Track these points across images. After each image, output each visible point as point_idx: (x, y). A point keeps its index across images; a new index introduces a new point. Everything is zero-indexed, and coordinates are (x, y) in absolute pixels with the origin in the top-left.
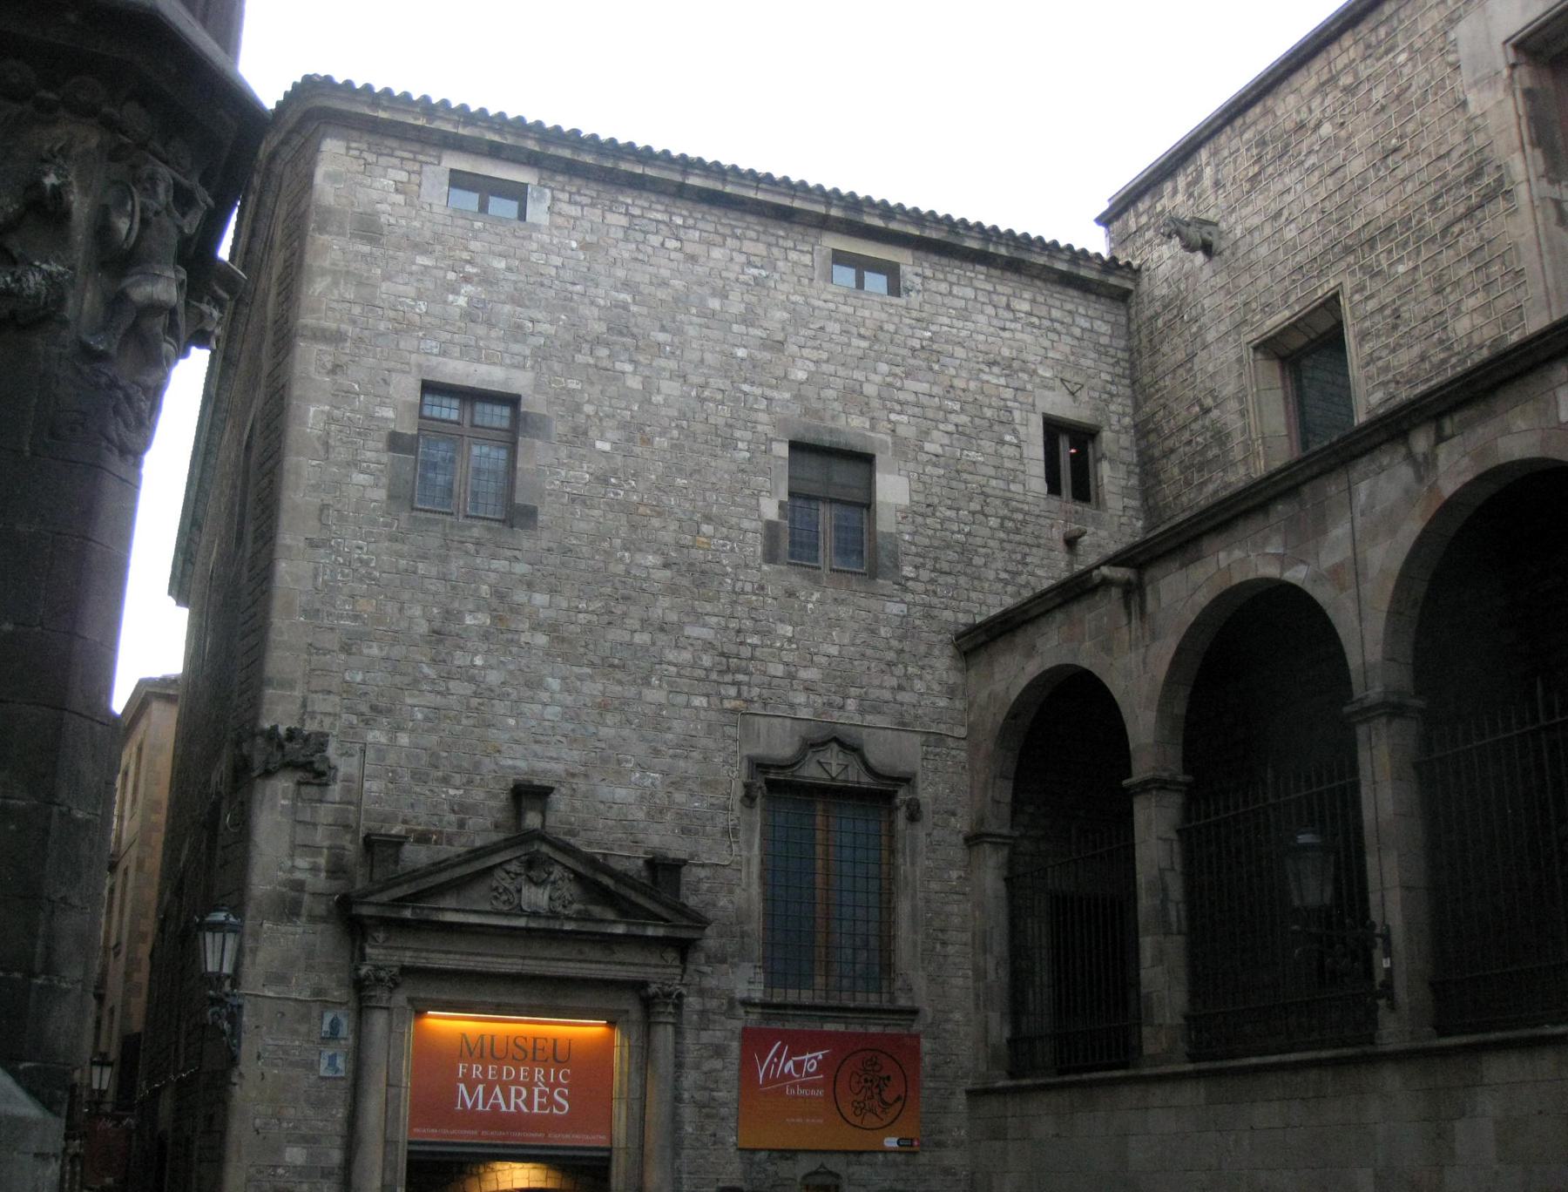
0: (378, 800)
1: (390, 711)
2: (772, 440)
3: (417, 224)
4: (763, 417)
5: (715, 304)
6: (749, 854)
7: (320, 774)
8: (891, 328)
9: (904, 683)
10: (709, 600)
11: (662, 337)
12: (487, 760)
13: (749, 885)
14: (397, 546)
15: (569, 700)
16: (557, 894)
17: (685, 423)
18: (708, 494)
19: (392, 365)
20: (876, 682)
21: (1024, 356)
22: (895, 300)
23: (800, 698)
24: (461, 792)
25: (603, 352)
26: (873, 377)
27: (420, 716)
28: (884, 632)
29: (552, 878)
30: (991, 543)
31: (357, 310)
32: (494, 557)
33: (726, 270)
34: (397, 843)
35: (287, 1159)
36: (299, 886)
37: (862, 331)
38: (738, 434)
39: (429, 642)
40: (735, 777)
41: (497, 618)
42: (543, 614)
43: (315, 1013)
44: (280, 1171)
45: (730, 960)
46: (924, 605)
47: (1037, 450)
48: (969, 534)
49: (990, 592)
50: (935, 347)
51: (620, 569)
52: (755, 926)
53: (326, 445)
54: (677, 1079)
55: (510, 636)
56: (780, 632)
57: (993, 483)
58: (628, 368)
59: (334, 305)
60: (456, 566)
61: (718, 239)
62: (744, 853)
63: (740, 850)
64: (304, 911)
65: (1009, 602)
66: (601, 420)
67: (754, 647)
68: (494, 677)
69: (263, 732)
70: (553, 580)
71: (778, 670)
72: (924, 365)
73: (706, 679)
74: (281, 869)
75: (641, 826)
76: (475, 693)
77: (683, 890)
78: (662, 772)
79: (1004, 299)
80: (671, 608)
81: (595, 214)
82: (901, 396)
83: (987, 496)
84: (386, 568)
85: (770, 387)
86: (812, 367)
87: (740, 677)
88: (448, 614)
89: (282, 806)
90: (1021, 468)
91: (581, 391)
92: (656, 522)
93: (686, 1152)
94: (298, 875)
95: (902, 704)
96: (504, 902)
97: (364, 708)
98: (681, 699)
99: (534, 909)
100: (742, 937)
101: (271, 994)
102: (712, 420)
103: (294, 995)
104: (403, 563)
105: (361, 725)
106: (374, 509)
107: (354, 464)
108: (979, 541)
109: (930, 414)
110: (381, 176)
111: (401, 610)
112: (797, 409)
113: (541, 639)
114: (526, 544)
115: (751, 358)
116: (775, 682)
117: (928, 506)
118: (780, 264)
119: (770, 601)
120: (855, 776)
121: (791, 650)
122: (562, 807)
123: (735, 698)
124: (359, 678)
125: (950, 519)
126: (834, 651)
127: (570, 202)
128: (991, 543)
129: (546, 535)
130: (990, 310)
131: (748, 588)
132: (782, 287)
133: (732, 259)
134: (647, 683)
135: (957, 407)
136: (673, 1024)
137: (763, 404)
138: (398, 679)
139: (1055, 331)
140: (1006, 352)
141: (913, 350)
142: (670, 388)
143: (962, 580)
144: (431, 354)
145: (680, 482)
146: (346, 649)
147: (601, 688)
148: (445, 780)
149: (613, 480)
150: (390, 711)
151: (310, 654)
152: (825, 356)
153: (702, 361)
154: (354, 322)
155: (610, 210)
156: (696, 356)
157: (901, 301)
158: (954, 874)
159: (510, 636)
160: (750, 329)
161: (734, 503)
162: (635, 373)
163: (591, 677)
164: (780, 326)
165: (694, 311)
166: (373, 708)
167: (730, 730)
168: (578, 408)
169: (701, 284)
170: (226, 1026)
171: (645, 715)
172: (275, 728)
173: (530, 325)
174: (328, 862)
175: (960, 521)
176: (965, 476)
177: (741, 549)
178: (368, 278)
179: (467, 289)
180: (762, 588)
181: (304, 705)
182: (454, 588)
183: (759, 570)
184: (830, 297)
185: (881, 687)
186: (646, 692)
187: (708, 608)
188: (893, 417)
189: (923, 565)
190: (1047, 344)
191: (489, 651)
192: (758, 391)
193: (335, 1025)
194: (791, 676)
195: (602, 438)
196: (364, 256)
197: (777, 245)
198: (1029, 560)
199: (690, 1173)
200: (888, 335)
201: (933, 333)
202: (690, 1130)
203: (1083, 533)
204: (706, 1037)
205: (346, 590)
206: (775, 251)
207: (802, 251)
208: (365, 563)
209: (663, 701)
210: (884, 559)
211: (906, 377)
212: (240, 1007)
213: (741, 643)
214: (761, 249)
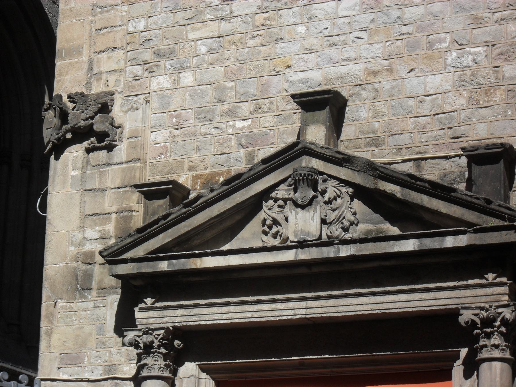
7: (102, 136)
16: (332, 216)
24: (249, 122)
27: (203, 49)
64: (94, 285)
74: (72, 244)
75: (462, 116)
78: (486, 44)
89: (73, 177)
105: (146, 74)
138: (180, 15)
148: (231, 113)
166: (159, 54)
174: (116, 228)
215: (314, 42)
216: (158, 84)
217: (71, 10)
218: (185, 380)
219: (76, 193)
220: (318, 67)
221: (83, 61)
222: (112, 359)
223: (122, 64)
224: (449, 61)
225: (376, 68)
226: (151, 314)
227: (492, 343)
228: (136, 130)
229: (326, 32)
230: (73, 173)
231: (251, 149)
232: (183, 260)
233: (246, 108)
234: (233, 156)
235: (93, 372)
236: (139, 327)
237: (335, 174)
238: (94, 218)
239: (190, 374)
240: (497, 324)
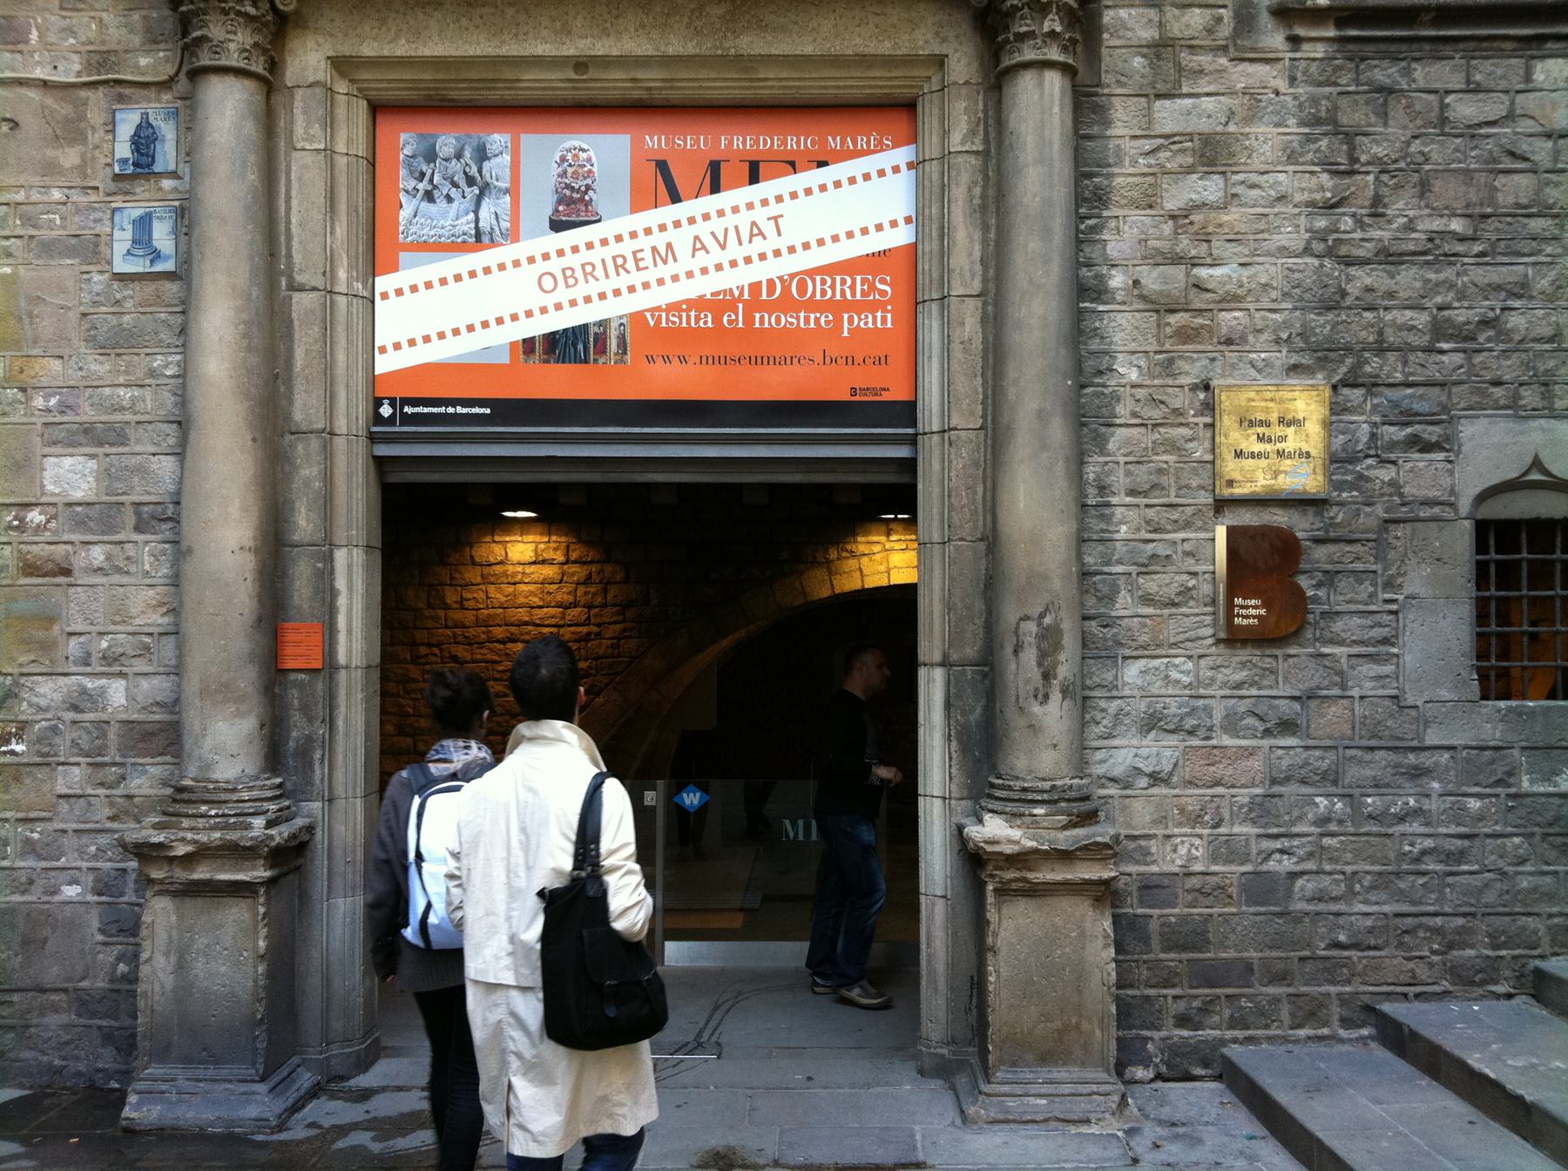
35: (50, 487)
43: (95, 116)
44: (35, 516)
93: (1121, 433)
103: (39, 73)
136: (1065, 68)
193: (144, 141)
199: (1132, 492)
202: (1134, 375)
204: (1169, 115)
218: (299, 94)
222: (107, 38)
227: (1046, 29)
235: (55, 67)
239: (311, 79)
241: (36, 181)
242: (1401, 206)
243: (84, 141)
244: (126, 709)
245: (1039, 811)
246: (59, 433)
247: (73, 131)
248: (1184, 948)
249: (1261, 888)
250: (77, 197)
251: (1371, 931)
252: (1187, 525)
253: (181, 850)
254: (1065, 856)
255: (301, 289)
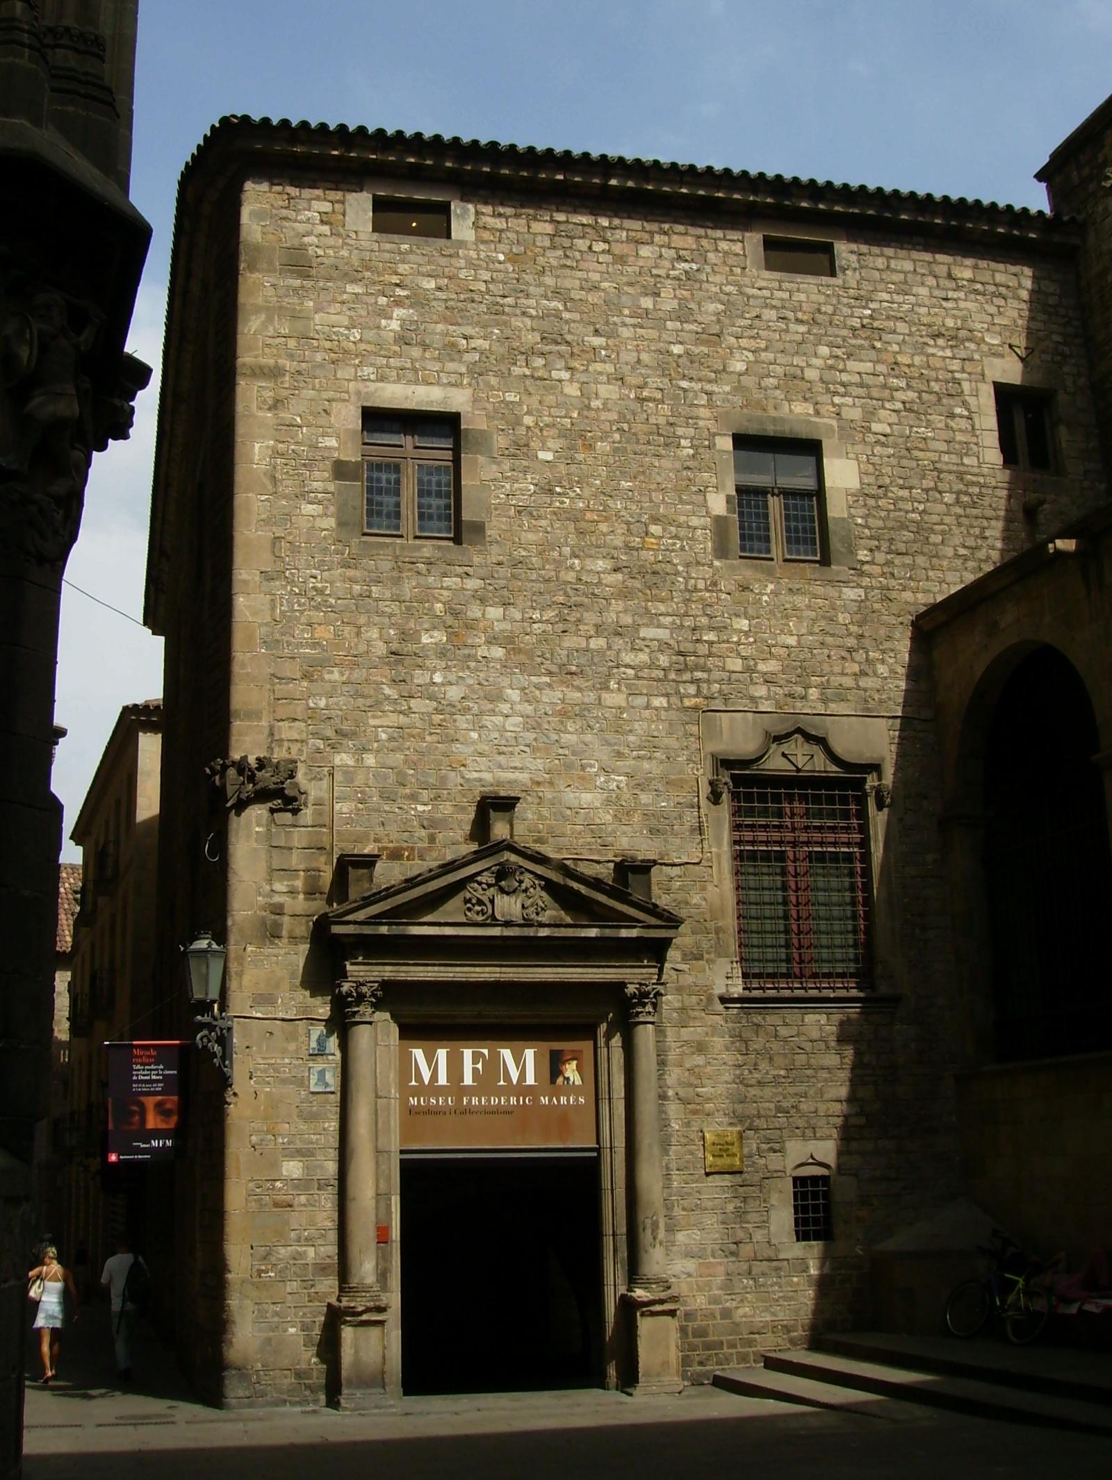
0: (349, 821)
1: (352, 735)
2: (714, 435)
3: (344, 253)
4: (703, 412)
5: (647, 303)
6: (720, 847)
8: (829, 309)
9: (865, 667)
10: (662, 601)
11: (597, 341)
12: (453, 774)
13: (720, 880)
14: (351, 573)
15: (529, 709)
17: (626, 426)
18: (653, 494)
19: (331, 394)
20: (837, 669)
21: (970, 324)
22: (831, 281)
23: (761, 691)
24: (430, 807)
25: (539, 362)
26: (814, 361)
27: (384, 736)
28: (842, 618)
29: (523, 886)
30: (947, 520)
31: (292, 343)
32: (445, 575)
33: (656, 267)
34: (368, 862)
35: (284, 1173)
36: (278, 910)
37: (800, 315)
38: (680, 431)
39: (388, 664)
40: (703, 774)
41: (452, 635)
42: (498, 627)
44: (278, 1184)
45: (706, 956)
46: (882, 588)
47: (989, 420)
48: (924, 511)
49: (949, 569)
50: (876, 324)
51: (571, 576)
52: (730, 922)
53: (274, 479)
54: (660, 1077)
55: (466, 651)
56: (736, 626)
57: (946, 458)
58: (565, 375)
59: (270, 341)
60: (408, 588)
61: (646, 237)
62: (713, 849)
63: (710, 847)
64: (284, 933)
65: (970, 578)
66: (541, 430)
67: (711, 643)
68: (454, 693)
69: (234, 763)
70: (505, 592)
71: (736, 664)
72: (866, 343)
73: (665, 679)
74: (260, 895)
75: (610, 829)
76: (436, 709)
77: (655, 890)
78: (627, 775)
79: (945, 268)
80: (626, 611)
81: (519, 224)
82: (845, 377)
83: (940, 471)
84: (340, 594)
85: (710, 382)
86: (751, 357)
87: (699, 675)
88: (405, 636)
90: (974, 440)
91: (520, 403)
92: (603, 527)
94: (277, 899)
95: (865, 690)
96: (478, 913)
97: (330, 732)
98: (641, 701)
99: (508, 918)
100: (717, 933)
101: (259, 1015)
102: (652, 420)
103: (281, 1015)
104: (357, 588)
105: (328, 749)
106: (325, 538)
107: (302, 495)
108: (935, 518)
109: (875, 393)
110: (305, 210)
111: (358, 634)
112: (738, 400)
113: (498, 652)
114: (476, 560)
115: (687, 353)
116: (734, 676)
117: (880, 487)
118: (711, 256)
119: (724, 596)
120: (820, 764)
121: (750, 644)
122: (530, 816)
123: (696, 696)
124: (322, 703)
125: (902, 499)
126: (792, 641)
127: (493, 216)
128: (947, 520)
129: (495, 549)
130: (931, 281)
131: (701, 585)
132: (718, 279)
133: (661, 256)
134: (606, 688)
135: (903, 384)
137: (703, 400)
138: (361, 701)
139: (1000, 295)
140: (950, 323)
141: (854, 329)
142: (608, 391)
143: (921, 560)
144: (369, 380)
145: (625, 484)
146: (306, 676)
147: (561, 696)
148: (414, 798)
149: (558, 489)
150: (354, 733)
151: (273, 685)
152: (763, 345)
153: (639, 361)
154: (291, 357)
155: (535, 219)
156: (632, 357)
157: (838, 281)
158: (929, 857)
159: (466, 651)
160: (685, 325)
161: (682, 502)
162: (571, 380)
163: (549, 685)
164: (714, 318)
165: (626, 312)
167: (694, 729)
168: (518, 422)
169: (631, 284)
170: (217, 1048)
171: (605, 719)
172: (245, 758)
173: (464, 342)
174: (305, 884)
175: (913, 500)
176: (916, 453)
177: (691, 548)
178: (301, 311)
179: (398, 312)
180: (715, 584)
181: (272, 734)
182: (408, 608)
183: (711, 565)
184: (763, 284)
185: (843, 674)
186: (605, 695)
187: (662, 608)
188: (837, 400)
189: (878, 548)
190: (993, 310)
191: (447, 667)
192: (697, 386)
194: (750, 670)
195: (544, 448)
196: (295, 290)
197: (706, 237)
198: (987, 534)
199: (678, 1170)
200: (826, 318)
201: (873, 310)
203: (1042, 502)
204: (686, 1033)
205: (303, 620)
206: (704, 242)
207: (731, 241)
208: (320, 592)
209: (624, 704)
210: (836, 544)
211: (848, 358)
212: (230, 1029)
213: (698, 641)
214: (690, 242)
215: (485, 748)
216: (341, 760)
217: (248, 674)
218: (379, 1024)
219: (262, 848)
220: (489, 770)
221: (262, 726)
223: (304, 736)
224: (598, 783)
225: (540, 779)
226: (362, 968)
228: (321, 798)
229: (496, 742)
230: (257, 829)
231: (432, 831)
232: (401, 927)
233: (425, 795)
234: (417, 834)
236: (350, 979)
237: (531, 869)
238: (282, 873)
240: (651, 996)
241: (280, 1055)
242: (764, 1065)
243: (297, 1040)
244: (315, 1259)
245: (654, 1286)
246: (287, 1152)
247: (292, 1037)
248: (700, 1337)
249: (726, 1313)
250: (294, 1062)
251: (763, 1327)
252: (697, 1182)
253: (360, 1309)
254: (661, 1302)
255: (381, 1097)
